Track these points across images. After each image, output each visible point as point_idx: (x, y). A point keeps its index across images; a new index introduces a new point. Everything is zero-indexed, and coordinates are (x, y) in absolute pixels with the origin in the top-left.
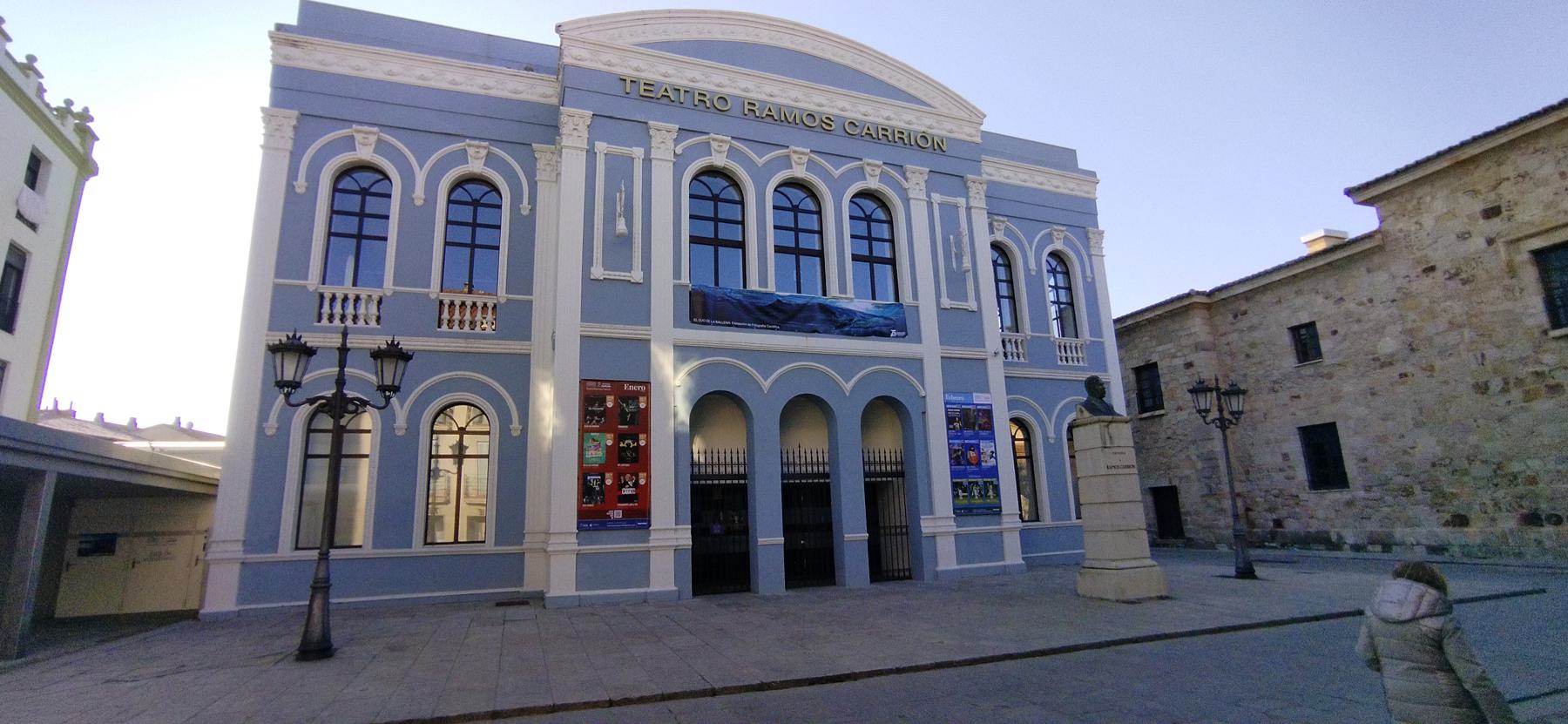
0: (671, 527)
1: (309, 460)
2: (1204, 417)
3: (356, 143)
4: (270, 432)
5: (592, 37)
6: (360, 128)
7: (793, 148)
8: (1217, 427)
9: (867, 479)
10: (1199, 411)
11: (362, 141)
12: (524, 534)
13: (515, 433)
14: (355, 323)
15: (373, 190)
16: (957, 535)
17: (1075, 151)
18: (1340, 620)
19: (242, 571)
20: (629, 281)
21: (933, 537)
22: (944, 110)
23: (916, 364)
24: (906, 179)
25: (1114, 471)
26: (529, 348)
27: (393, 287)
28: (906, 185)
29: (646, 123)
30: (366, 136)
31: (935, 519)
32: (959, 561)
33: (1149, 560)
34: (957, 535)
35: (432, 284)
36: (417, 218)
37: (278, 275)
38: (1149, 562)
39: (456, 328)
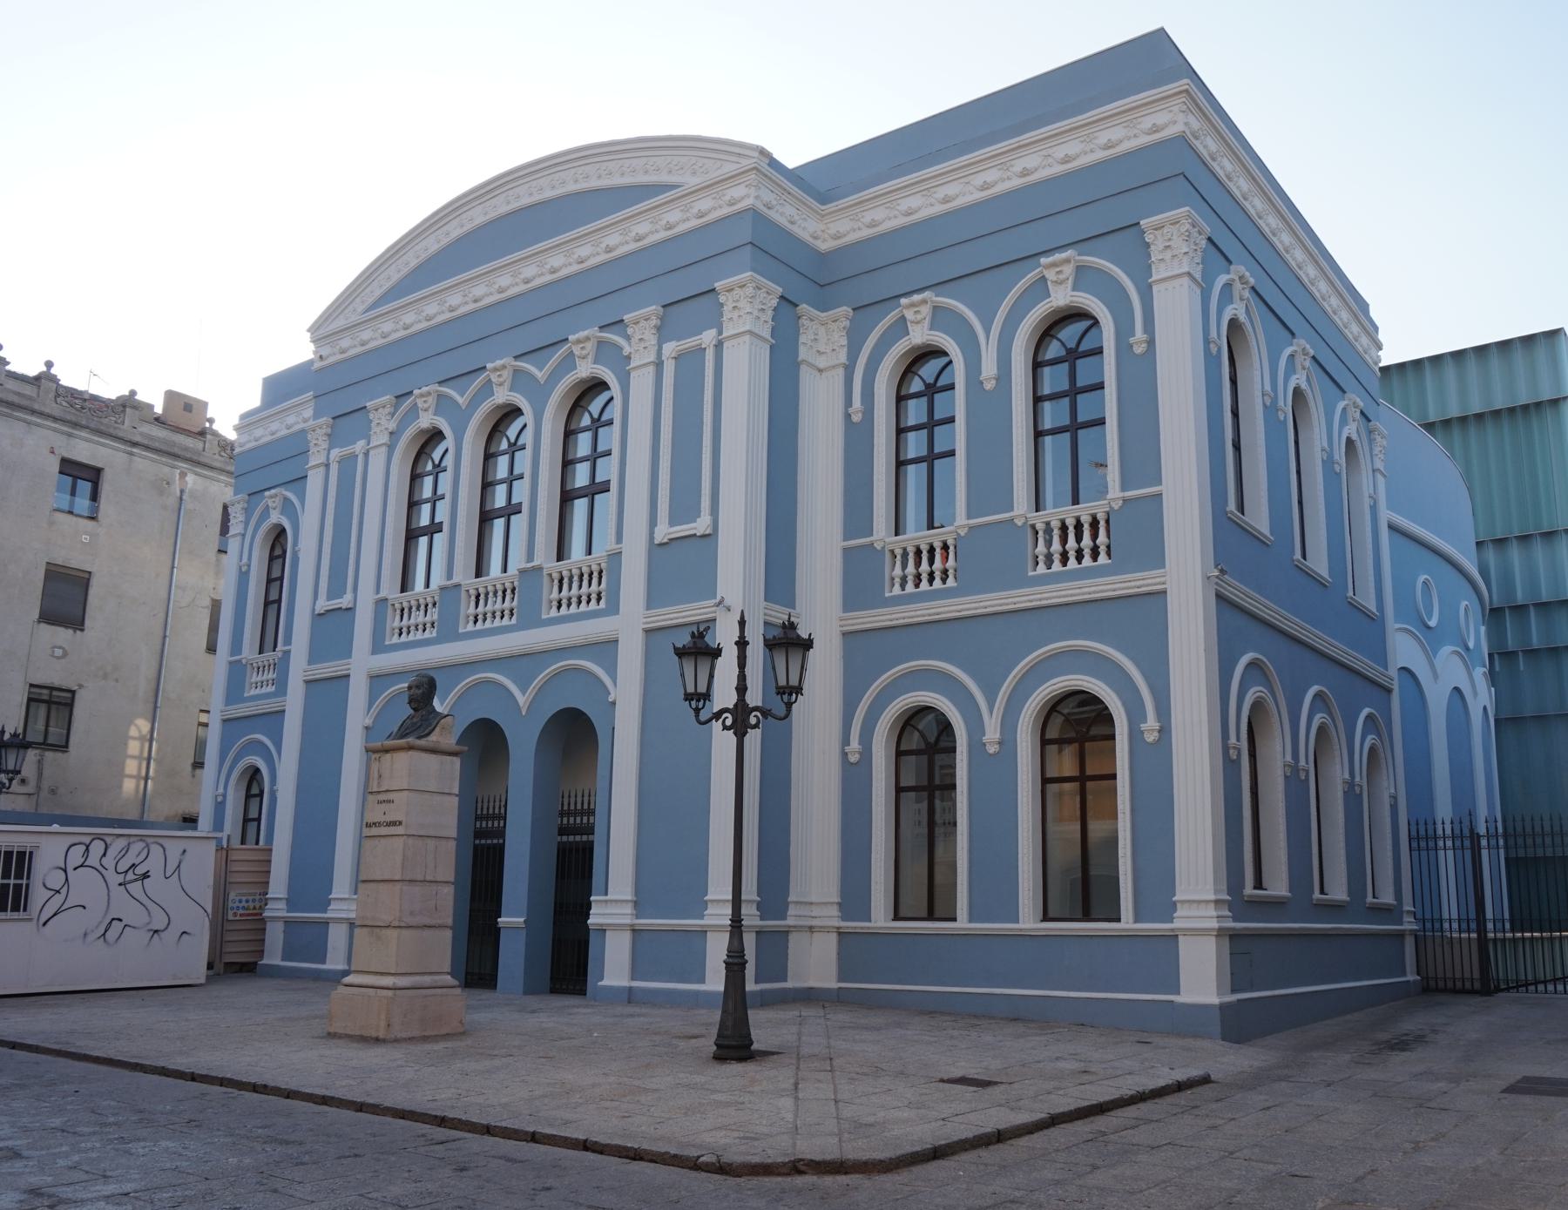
0: (832, 900)
1: (903, 795)
2: (697, 711)
3: (1049, 283)
4: (853, 758)
5: (340, 323)
6: (1050, 259)
7: (416, 392)
8: (725, 728)
9: (477, 842)
10: (688, 697)
11: (1055, 279)
12: (1175, 904)
13: (1151, 738)
14: (1080, 563)
15: (1083, 348)
16: (842, 934)
17: (1162, 29)
18: (842, 1179)
19: (840, 942)
20: (340, 608)
21: (602, 931)
22: (692, 181)
23: (606, 649)
24: (628, 338)
25: (374, 831)
26: (1162, 579)
27: (1121, 495)
28: (627, 350)
29: (366, 407)
30: (1058, 269)
31: (606, 901)
32: (840, 980)
33: (449, 977)
34: (842, 934)
35: (1015, 505)
36: (991, 405)
37: (846, 538)
38: (449, 979)
39: (1087, 561)
